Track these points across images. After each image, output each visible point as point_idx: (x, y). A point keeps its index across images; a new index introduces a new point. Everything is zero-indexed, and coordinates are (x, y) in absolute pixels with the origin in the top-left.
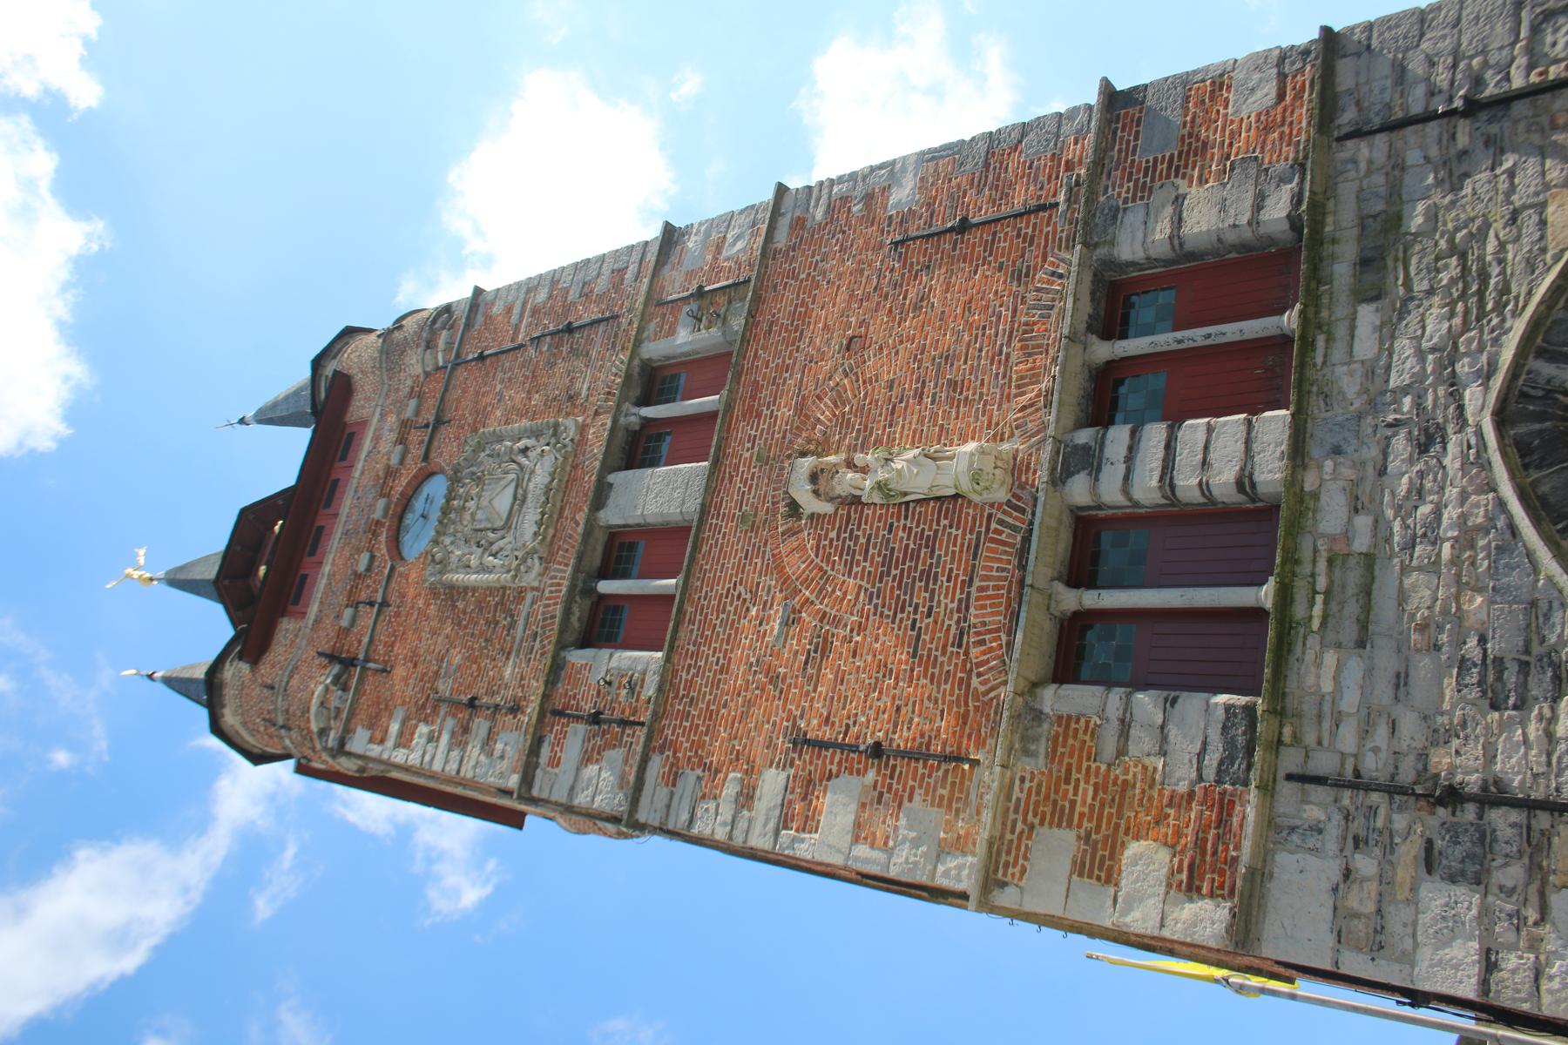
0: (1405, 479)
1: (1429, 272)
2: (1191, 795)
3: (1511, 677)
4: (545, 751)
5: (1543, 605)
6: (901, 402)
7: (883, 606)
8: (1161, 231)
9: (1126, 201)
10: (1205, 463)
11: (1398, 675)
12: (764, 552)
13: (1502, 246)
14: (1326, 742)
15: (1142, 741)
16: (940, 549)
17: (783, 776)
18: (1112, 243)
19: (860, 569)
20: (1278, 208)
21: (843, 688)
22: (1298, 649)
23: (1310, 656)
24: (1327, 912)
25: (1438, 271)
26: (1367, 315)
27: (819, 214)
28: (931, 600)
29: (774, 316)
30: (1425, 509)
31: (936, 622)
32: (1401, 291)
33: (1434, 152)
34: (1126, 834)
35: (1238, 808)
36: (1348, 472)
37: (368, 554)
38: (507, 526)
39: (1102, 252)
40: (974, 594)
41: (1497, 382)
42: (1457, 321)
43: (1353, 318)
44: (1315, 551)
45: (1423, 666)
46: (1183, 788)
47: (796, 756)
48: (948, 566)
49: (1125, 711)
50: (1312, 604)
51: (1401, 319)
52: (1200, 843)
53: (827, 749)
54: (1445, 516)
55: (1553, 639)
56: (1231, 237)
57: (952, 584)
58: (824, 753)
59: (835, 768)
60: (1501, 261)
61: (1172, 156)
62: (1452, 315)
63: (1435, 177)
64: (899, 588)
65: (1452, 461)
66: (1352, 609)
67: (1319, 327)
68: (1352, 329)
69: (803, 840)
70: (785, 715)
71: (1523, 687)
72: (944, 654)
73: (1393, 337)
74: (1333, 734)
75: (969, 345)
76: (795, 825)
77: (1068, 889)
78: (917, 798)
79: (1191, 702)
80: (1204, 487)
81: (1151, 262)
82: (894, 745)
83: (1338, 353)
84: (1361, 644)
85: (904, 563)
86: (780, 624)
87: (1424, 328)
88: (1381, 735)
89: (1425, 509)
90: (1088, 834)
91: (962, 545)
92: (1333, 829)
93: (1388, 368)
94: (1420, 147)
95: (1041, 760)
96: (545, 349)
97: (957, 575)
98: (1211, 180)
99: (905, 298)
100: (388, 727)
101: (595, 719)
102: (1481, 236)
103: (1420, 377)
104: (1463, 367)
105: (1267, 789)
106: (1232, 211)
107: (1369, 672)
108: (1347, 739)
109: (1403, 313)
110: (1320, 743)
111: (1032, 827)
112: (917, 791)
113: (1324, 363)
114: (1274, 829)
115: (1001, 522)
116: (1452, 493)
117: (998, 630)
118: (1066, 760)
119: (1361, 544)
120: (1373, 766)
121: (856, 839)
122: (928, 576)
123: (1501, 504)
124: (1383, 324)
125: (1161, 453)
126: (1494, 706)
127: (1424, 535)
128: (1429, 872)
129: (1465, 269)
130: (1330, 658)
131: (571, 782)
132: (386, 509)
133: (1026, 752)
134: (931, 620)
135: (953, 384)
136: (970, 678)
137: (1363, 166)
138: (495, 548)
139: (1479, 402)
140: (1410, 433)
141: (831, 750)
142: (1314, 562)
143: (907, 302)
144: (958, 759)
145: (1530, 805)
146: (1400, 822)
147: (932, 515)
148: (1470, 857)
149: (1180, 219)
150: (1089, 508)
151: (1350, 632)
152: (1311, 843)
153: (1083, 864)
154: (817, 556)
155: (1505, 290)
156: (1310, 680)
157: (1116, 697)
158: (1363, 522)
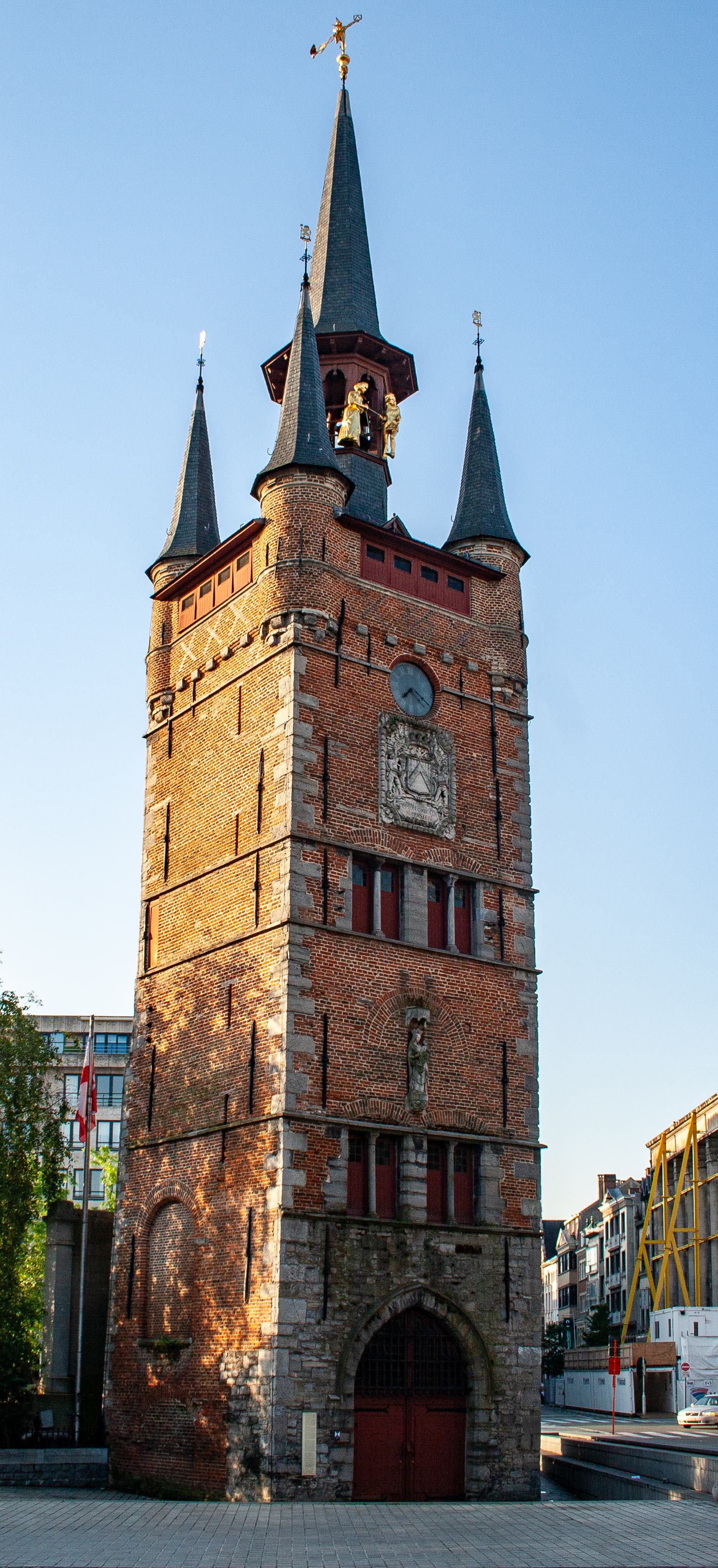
12: (391, 987)
21: (344, 1039)
27: (524, 999)
28: (375, 1080)
29: (485, 977)
31: (367, 1083)
34: (308, 1171)
37: (394, 642)
38: (408, 790)
47: (320, 1018)
59: (316, 1038)
64: (379, 1064)
72: (357, 1088)
80: (406, 1192)
85: (387, 1065)
90: (307, 1156)
96: (491, 796)
100: (308, 692)
138: (398, 780)
153: (299, 1155)
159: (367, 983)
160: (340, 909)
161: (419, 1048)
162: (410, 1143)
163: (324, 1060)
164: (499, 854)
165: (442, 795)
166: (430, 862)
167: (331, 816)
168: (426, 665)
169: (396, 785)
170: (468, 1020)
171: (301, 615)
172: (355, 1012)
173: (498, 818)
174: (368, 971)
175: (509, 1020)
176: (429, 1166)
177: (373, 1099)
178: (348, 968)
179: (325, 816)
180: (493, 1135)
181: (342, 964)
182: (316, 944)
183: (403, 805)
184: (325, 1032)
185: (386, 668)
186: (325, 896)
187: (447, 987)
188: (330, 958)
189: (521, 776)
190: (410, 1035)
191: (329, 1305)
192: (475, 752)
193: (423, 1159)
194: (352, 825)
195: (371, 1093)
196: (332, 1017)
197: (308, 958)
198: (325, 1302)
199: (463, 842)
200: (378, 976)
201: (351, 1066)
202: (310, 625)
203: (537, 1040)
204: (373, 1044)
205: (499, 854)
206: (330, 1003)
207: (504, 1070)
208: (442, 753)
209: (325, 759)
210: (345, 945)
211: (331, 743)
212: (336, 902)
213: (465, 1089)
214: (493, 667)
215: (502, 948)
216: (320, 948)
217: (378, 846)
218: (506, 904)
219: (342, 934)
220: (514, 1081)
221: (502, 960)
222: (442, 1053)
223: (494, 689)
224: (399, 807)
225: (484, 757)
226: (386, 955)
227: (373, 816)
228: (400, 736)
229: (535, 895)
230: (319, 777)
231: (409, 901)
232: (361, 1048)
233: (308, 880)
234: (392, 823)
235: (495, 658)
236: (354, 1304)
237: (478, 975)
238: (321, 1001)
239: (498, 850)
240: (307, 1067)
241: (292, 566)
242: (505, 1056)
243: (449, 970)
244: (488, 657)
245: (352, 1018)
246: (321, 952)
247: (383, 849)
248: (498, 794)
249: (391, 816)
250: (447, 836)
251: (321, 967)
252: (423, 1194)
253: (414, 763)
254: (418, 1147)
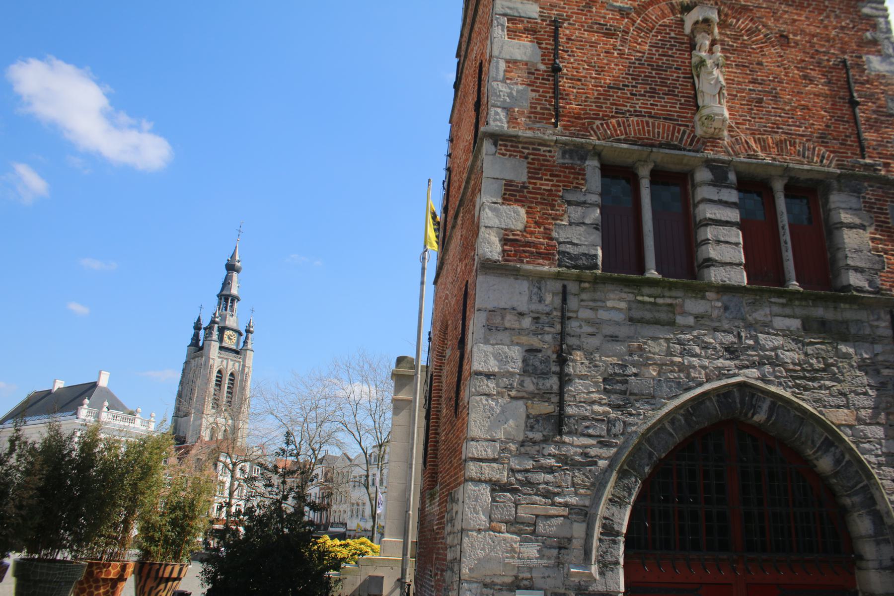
0: (712, 341)
1: (817, 354)
2: (551, 239)
3: (618, 387)
5: (653, 401)
6: (750, 71)
7: (635, 67)
8: (846, 217)
9: (864, 197)
10: (719, 242)
11: (616, 337)
13: (828, 388)
14: (582, 303)
15: (575, 213)
16: (668, 99)
17: (536, 15)
18: (840, 190)
19: (654, 52)
20: (855, 279)
21: (588, 47)
22: (627, 290)
23: (624, 295)
24: (502, 305)
25: (817, 358)
26: (795, 324)
28: (640, 95)
30: (697, 350)
31: (628, 98)
32: (807, 340)
33: (880, 358)
35: (547, 262)
36: (715, 314)
39: (835, 184)
40: (644, 119)
41: (760, 384)
42: (791, 367)
43: (794, 317)
44: (676, 298)
45: (622, 348)
46: (554, 234)
47: (548, 22)
48: (659, 104)
49: (590, 204)
50: (649, 296)
51: (793, 340)
52: (528, 244)
53: (554, 40)
54: (694, 359)
55: (637, 405)
56: (840, 255)
57: (649, 106)
58: (552, 39)
59: (544, 46)
60: (820, 388)
61: (888, 223)
62: (794, 364)
63: (866, 358)
64: (645, 76)
65: (721, 362)
66: (648, 315)
67: (790, 300)
68: (788, 316)
69: (503, 31)
70: (569, 14)
71: (615, 392)
72: (611, 104)
73: (784, 336)
74: (586, 307)
75: (783, 109)
76: (510, 25)
77: (497, 179)
78: (534, 94)
79: (596, 237)
80: (706, 241)
81: (828, 212)
82: (560, 79)
83: (776, 309)
84: (631, 320)
85: (659, 78)
86: (620, 6)
87: (788, 351)
88: (587, 329)
89: (697, 350)
90: (526, 188)
91: (671, 111)
92: (541, 307)
93: (768, 333)
94: (883, 352)
95: (561, 161)
97: (654, 109)
98: (873, 245)
99: (811, 69)
102: (834, 378)
103: (763, 349)
104: (767, 369)
105: (558, 276)
106: (855, 255)
107: (617, 323)
108: (585, 314)
109: (796, 341)
110: (582, 300)
111: (526, 158)
112: (537, 94)
113: (771, 302)
114: (540, 279)
115: (684, 132)
116: (706, 362)
117: (626, 134)
118: (562, 174)
119: (680, 320)
120: (573, 326)
121: (508, 61)
122: (653, 92)
123: (700, 384)
124: (791, 331)
125: (723, 219)
126: (605, 380)
127: (685, 349)
128: (526, 351)
129: (817, 371)
130: (623, 305)
133: (564, 153)
134: (629, 95)
135: (760, 101)
136: (599, 119)
137: (876, 323)
139: (751, 375)
140: (735, 343)
141: (553, 43)
142: (670, 297)
143: (808, 71)
144: (557, 116)
145: (561, 393)
146: (548, 338)
147: (687, 93)
148: (535, 368)
149: (852, 228)
150: (693, 180)
151: (636, 314)
152: (534, 298)
153: (511, 186)
154: (660, 25)
155: (806, 389)
156: (612, 296)
157: (595, 198)
158: (691, 321)
213: (789, 110)
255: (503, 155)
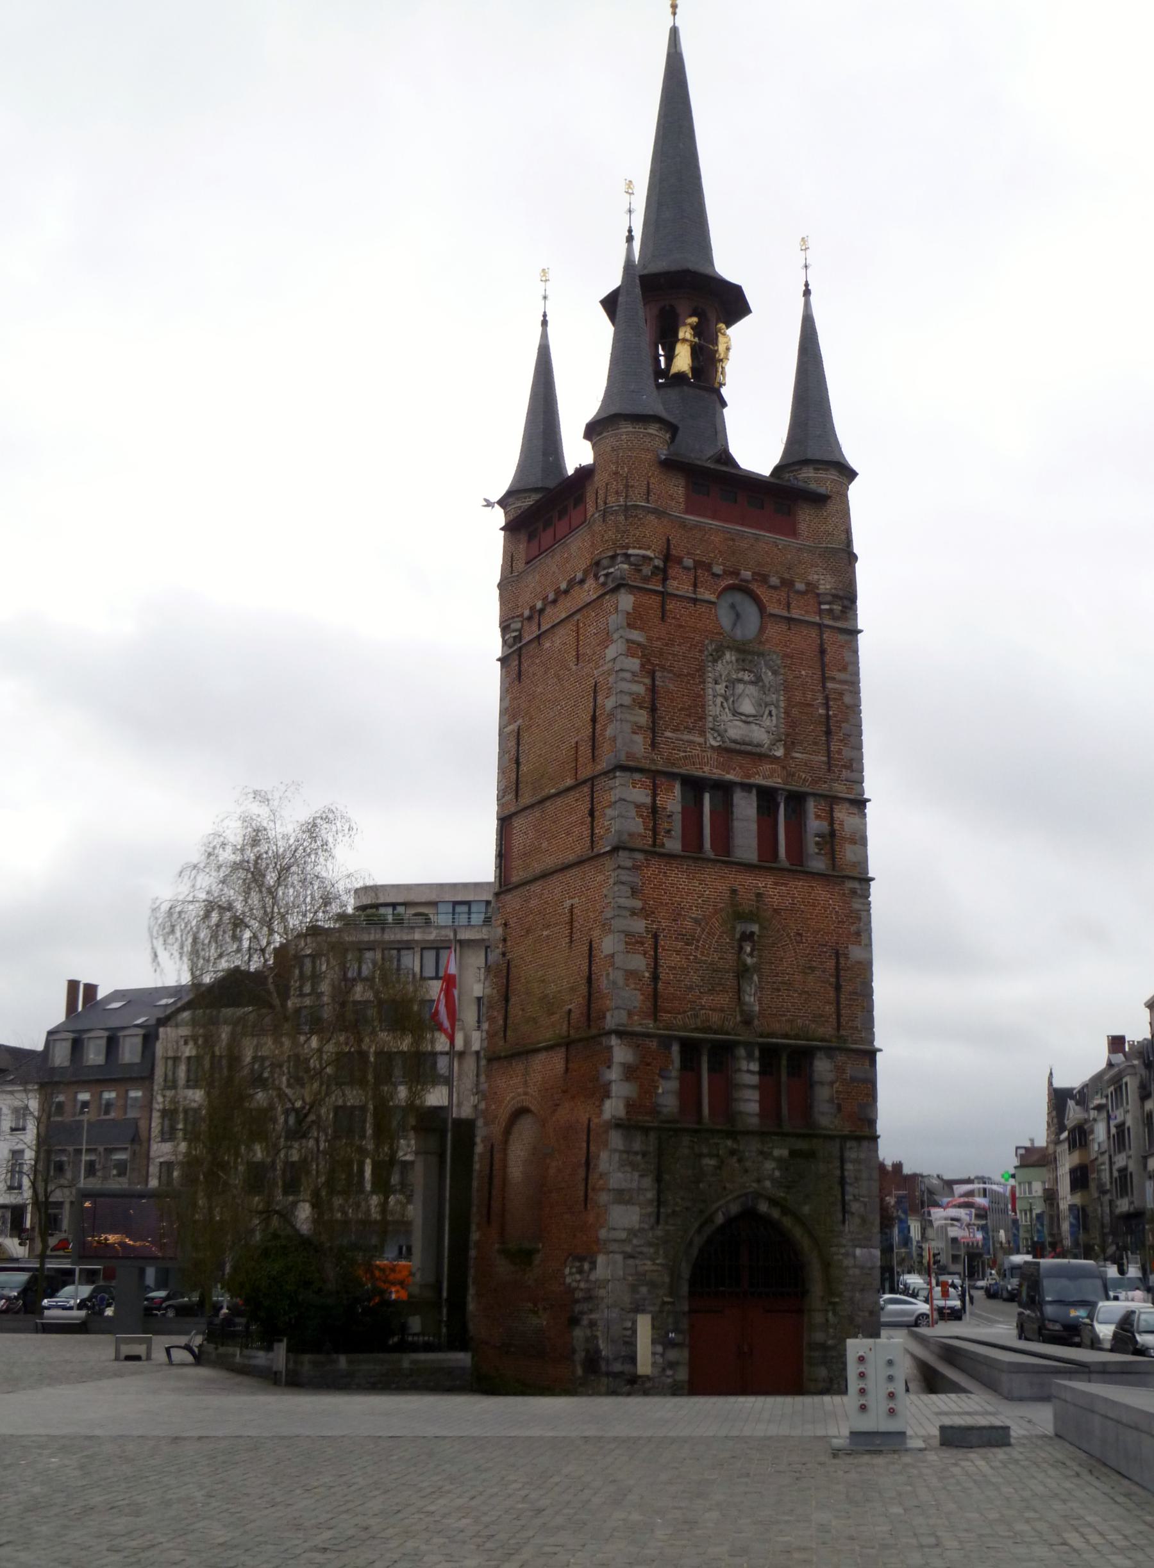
4: (637, 776)
28: (705, 993)
38: (735, 713)
100: (635, 628)
101: (654, 810)
131: (628, 799)
132: (746, 581)
138: (725, 704)
159: (696, 900)
160: (669, 831)
161: (749, 961)
162: (742, 1052)
163: (655, 977)
164: (830, 767)
165: (770, 714)
166: (759, 780)
167: (659, 744)
168: (753, 590)
169: (724, 709)
170: (799, 930)
171: (627, 556)
172: (686, 928)
173: (828, 733)
174: (697, 889)
175: (841, 928)
176: (762, 1073)
177: (704, 1011)
178: (677, 888)
179: (653, 745)
180: (826, 1041)
181: (671, 884)
182: (645, 867)
183: (730, 727)
184: (656, 949)
185: (713, 598)
186: (655, 820)
187: (777, 899)
188: (660, 879)
189: (851, 688)
190: (741, 949)
191: (662, 1210)
192: (804, 670)
193: (755, 1066)
194: (679, 751)
195: (701, 1005)
196: (662, 935)
197: (636, 880)
198: (658, 1206)
199: (793, 758)
200: (707, 893)
201: (682, 981)
202: (635, 565)
203: (871, 945)
204: (704, 958)
205: (830, 767)
206: (660, 922)
207: (838, 977)
208: (770, 674)
209: (653, 689)
210: (675, 865)
211: (658, 674)
212: (666, 826)
213: (797, 997)
214: (821, 587)
215: (833, 859)
216: (649, 870)
217: (706, 769)
218: (837, 814)
219: (670, 857)
220: (847, 988)
221: (833, 869)
222: (773, 963)
223: (823, 607)
224: (726, 731)
225: (813, 673)
226: (715, 872)
227: (701, 740)
228: (727, 662)
229: (867, 804)
230: (646, 708)
231: (737, 819)
232: (691, 963)
233: (638, 806)
234: (720, 746)
235: (822, 577)
236: (687, 1209)
237: (809, 886)
238: (652, 921)
239: (829, 763)
240: (639, 984)
241: (619, 510)
242: (838, 963)
243: (778, 883)
244: (816, 577)
245: (683, 935)
246: (651, 874)
247: (710, 770)
248: (828, 708)
249: (719, 739)
250: (776, 753)
251: (651, 888)
252: (755, 1101)
253: (741, 687)
254: (750, 1057)
255: (625, 1045)
